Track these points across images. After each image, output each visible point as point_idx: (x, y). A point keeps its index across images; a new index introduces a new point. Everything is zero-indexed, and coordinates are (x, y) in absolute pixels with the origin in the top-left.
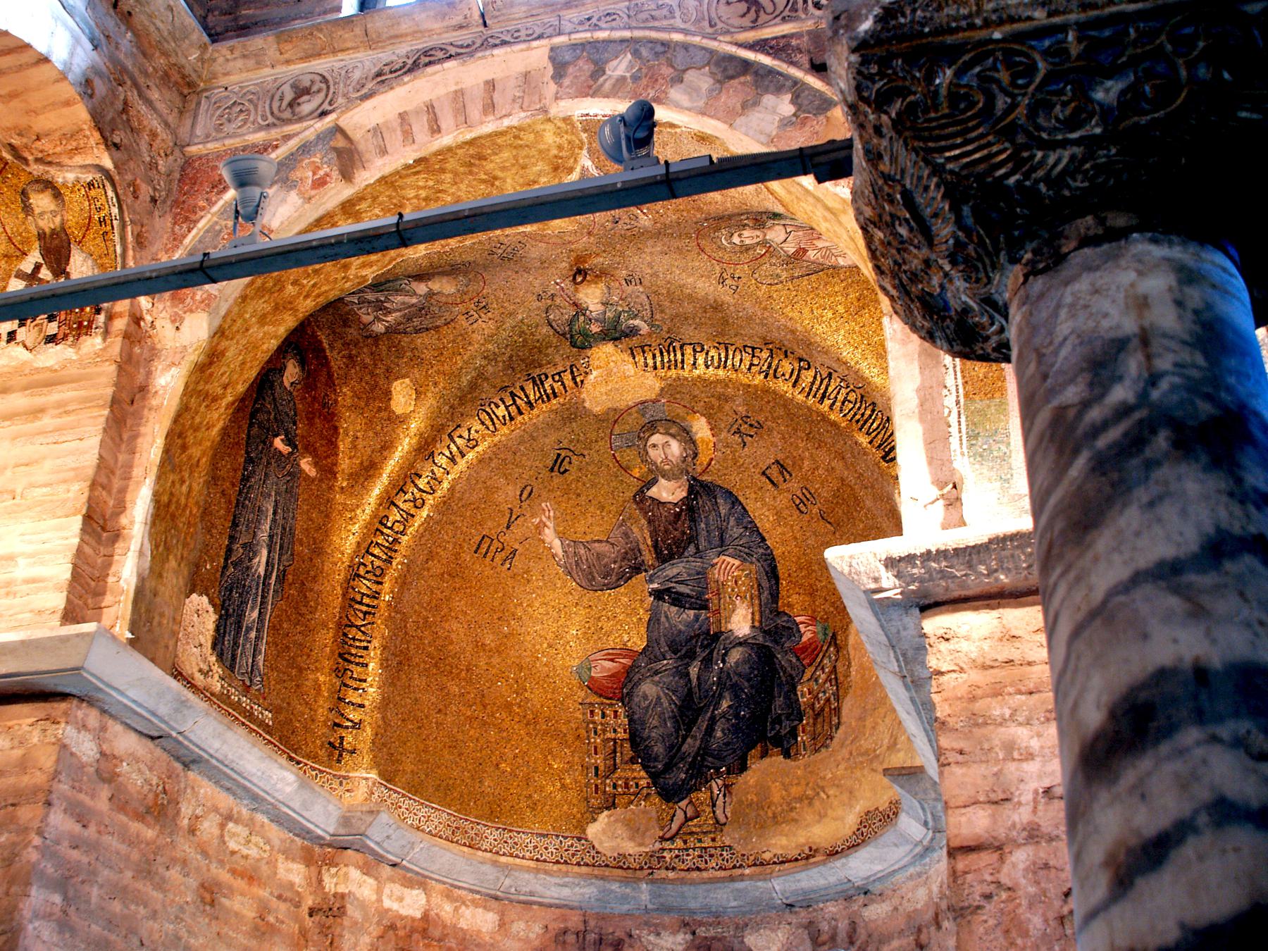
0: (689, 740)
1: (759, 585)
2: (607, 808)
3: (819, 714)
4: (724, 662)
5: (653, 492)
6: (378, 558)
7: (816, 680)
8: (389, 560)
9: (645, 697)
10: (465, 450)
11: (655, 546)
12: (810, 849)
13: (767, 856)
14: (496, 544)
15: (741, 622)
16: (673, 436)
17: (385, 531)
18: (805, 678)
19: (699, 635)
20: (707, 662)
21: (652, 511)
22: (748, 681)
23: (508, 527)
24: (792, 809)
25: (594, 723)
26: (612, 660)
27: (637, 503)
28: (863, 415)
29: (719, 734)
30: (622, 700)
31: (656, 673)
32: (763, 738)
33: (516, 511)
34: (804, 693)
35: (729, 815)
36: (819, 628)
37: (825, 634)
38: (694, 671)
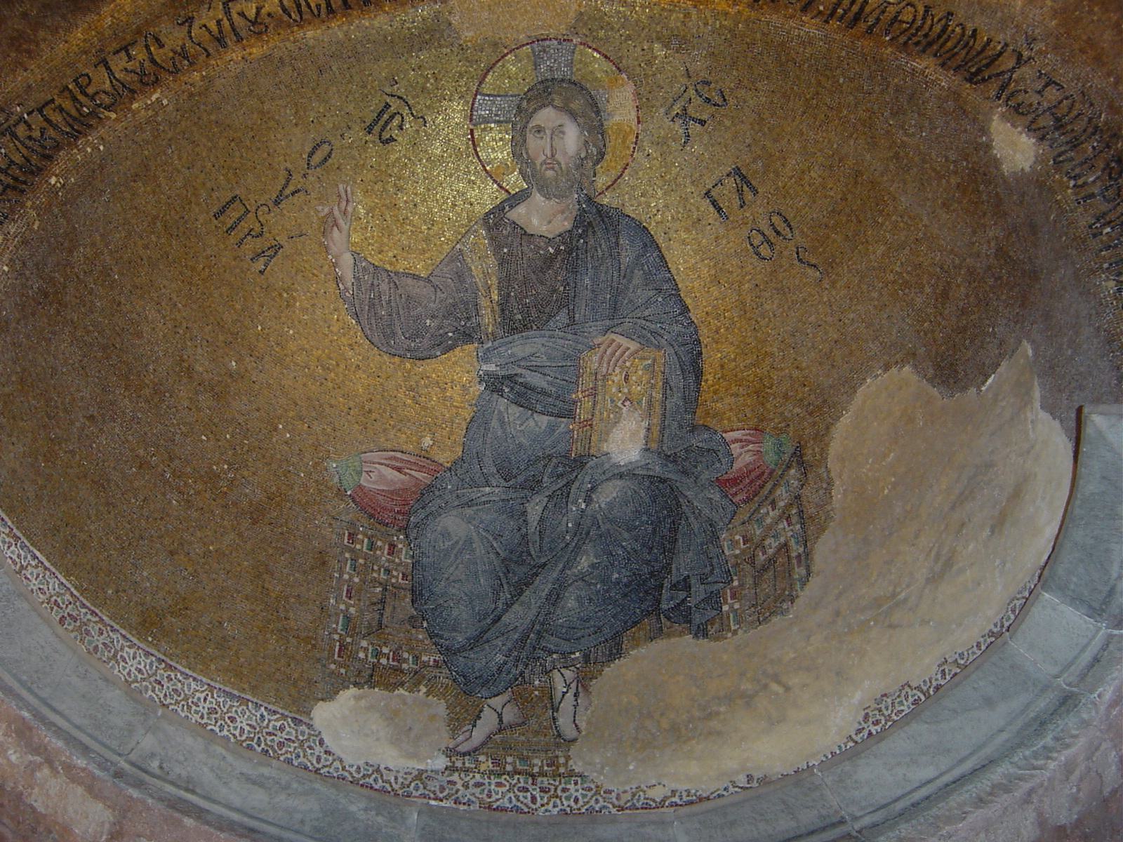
0: (516, 607)
1: (666, 383)
2: (356, 684)
3: (764, 569)
4: (588, 500)
5: (518, 213)
6: (55, 127)
7: (760, 521)
8: (76, 134)
9: (446, 535)
10: (243, 34)
11: (505, 298)
12: (750, 778)
13: (657, 794)
14: (249, 223)
15: (626, 443)
16: (573, 115)
17: (81, 97)
18: (737, 521)
19: (550, 457)
20: (561, 497)
21: (510, 246)
22: (629, 530)
23: (277, 203)
24: (710, 716)
25: (352, 551)
26: (399, 470)
27: (489, 229)
28: (926, 36)
29: (571, 603)
30: (405, 529)
31: (470, 503)
32: (656, 610)
33: (297, 179)
34: (732, 545)
35: (583, 725)
36: (768, 445)
37: (779, 453)
38: (535, 510)
